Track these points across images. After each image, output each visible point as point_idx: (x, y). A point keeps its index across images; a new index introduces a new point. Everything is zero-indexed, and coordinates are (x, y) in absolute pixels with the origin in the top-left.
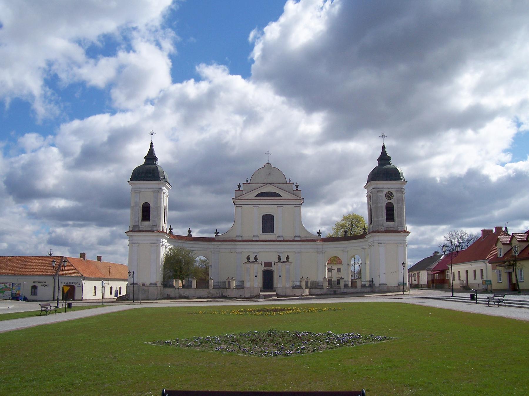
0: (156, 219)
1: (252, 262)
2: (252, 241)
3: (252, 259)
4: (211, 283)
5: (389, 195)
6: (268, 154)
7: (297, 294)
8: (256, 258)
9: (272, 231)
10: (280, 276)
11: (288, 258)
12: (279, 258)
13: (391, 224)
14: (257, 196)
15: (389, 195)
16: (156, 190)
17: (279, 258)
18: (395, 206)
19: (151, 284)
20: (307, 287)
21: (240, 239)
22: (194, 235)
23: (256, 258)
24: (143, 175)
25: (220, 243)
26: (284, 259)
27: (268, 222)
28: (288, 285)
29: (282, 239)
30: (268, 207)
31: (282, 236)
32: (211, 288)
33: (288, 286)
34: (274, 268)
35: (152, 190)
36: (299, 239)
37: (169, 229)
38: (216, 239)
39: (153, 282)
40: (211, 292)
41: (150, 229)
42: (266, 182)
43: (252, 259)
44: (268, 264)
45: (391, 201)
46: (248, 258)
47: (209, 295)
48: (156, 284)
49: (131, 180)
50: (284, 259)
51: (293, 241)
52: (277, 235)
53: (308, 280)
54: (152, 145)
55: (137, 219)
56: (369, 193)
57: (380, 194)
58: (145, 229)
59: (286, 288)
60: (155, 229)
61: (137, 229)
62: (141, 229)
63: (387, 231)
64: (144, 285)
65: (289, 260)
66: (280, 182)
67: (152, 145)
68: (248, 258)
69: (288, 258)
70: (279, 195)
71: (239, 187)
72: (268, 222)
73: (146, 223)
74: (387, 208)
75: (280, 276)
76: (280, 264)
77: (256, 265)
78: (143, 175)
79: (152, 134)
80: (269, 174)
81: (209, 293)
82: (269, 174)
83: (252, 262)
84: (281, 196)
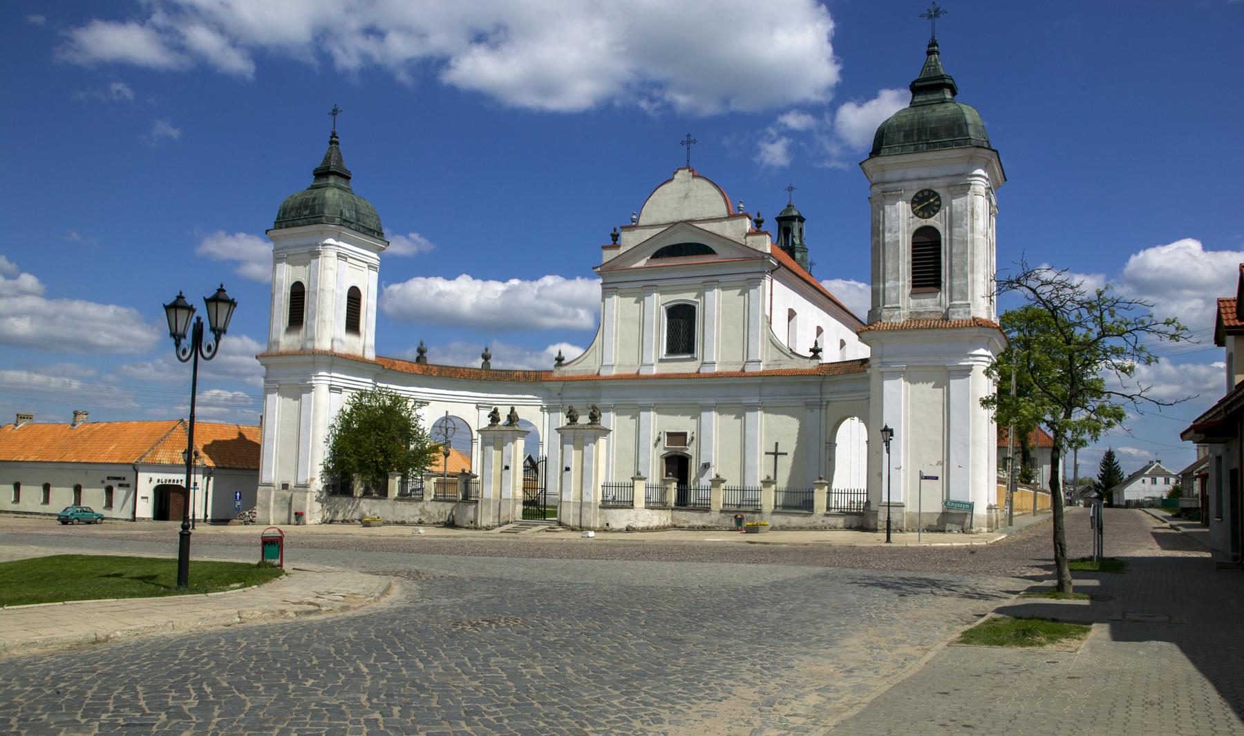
7: (614, 525)
14: (656, 256)
18: (944, 236)
27: (683, 329)
40: (428, 508)
47: (423, 519)
71: (615, 237)
72: (683, 329)
74: (915, 245)
81: (423, 512)
82: (686, 196)
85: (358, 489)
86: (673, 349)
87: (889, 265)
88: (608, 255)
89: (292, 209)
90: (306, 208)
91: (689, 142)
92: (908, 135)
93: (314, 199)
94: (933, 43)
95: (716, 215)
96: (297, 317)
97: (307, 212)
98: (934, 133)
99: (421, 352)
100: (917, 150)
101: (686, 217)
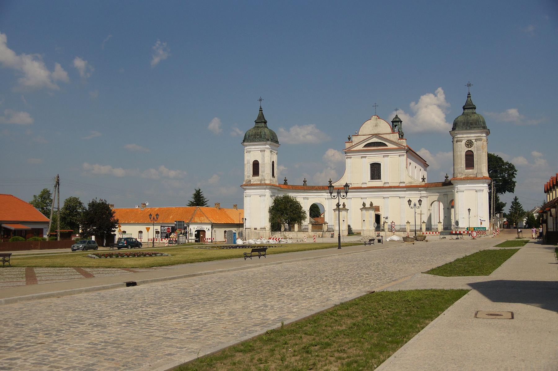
2: (361, 188)
5: (469, 143)
9: (379, 178)
14: (365, 146)
15: (469, 143)
17: (364, 204)
18: (475, 153)
19: (261, 228)
26: (368, 205)
27: (376, 171)
29: (387, 185)
30: (376, 158)
35: (260, 149)
41: (259, 182)
42: (372, 133)
45: (469, 149)
49: (244, 141)
52: (383, 182)
54: (261, 110)
57: (459, 143)
59: (370, 231)
60: (263, 182)
64: (255, 229)
66: (385, 132)
67: (261, 110)
71: (349, 139)
72: (376, 171)
73: (256, 178)
74: (466, 155)
76: (364, 211)
79: (260, 100)
80: (376, 126)
82: (376, 126)
84: (386, 145)
85: (283, 229)
87: (459, 161)
88: (348, 145)
90: (258, 135)
92: (464, 124)
93: (261, 132)
94: (469, 94)
95: (387, 132)
96: (256, 172)
98: (472, 124)
99: (285, 181)
100: (466, 129)
101: (376, 133)
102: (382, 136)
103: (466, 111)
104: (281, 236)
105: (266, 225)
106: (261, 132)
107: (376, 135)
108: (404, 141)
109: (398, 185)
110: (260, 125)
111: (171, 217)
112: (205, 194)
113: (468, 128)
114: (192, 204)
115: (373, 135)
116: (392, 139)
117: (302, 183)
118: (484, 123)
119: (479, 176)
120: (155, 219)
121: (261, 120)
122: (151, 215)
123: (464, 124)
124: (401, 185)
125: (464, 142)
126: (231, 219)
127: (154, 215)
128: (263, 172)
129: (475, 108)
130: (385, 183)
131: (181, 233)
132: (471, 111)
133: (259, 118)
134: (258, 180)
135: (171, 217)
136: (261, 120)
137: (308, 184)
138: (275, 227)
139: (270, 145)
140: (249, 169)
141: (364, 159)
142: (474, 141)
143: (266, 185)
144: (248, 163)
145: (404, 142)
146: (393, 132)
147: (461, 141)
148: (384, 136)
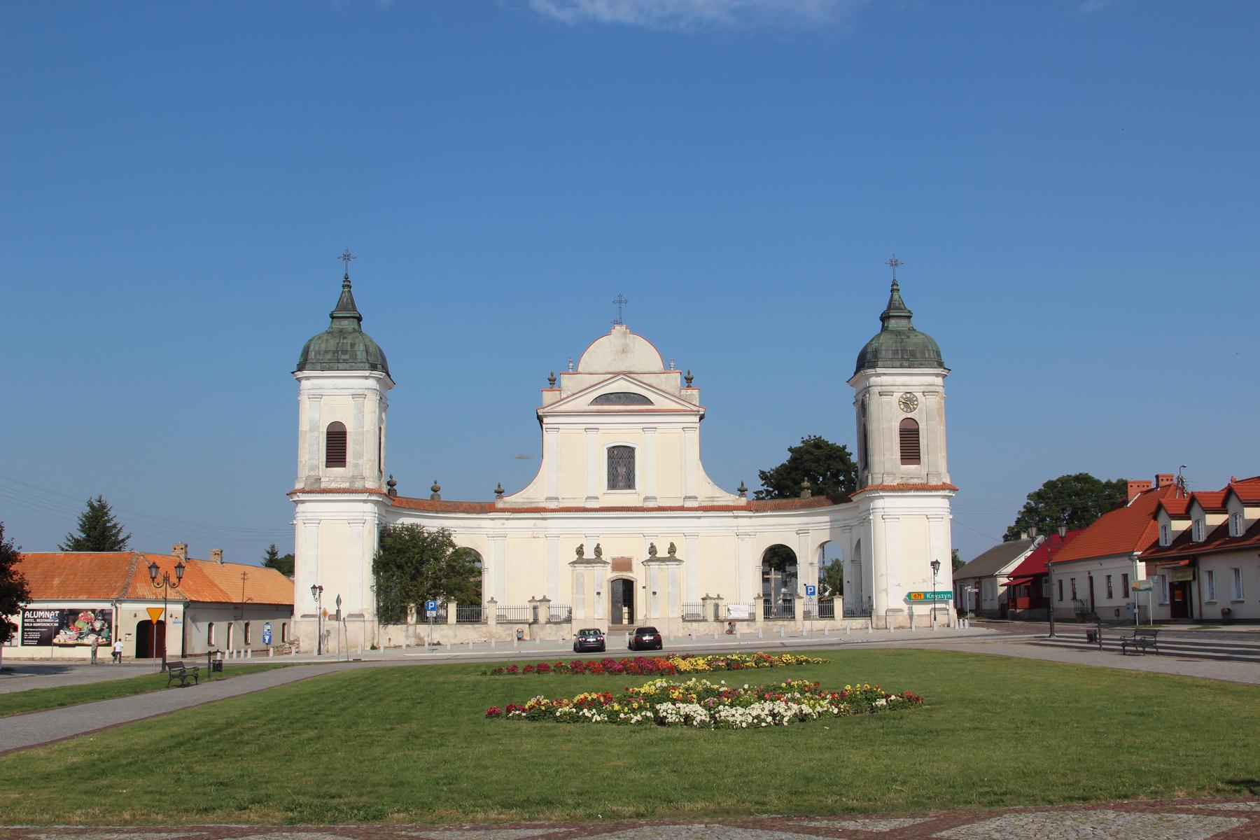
0: (361, 462)
1: (589, 562)
3: (589, 554)
4: (489, 611)
5: (908, 402)
6: (620, 302)
8: (598, 551)
9: (630, 484)
10: (654, 593)
11: (672, 549)
12: (653, 550)
13: (912, 468)
14: (597, 401)
15: (908, 402)
16: (360, 392)
17: (653, 550)
18: (922, 427)
20: (717, 619)
21: (553, 505)
22: (445, 495)
23: (598, 551)
24: (329, 356)
25: (507, 515)
26: (662, 552)
27: (621, 465)
28: (677, 613)
29: (651, 504)
31: (655, 498)
32: (492, 622)
33: (671, 616)
34: (638, 575)
36: (695, 504)
37: (389, 484)
38: (500, 505)
39: (357, 612)
41: (346, 485)
43: (589, 554)
44: (623, 564)
45: (909, 415)
46: (580, 551)
48: (362, 615)
50: (662, 552)
51: (682, 509)
53: (719, 602)
54: (347, 285)
55: (315, 462)
56: (860, 397)
57: (884, 398)
58: (333, 486)
59: (670, 620)
60: (358, 485)
61: (316, 487)
62: (323, 486)
63: (904, 488)
65: (677, 555)
66: (646, 370)
67: (347, 285)
68: (580, 551)
69: (672, 549)
70: (647, 401)
71: (552, 381)
72: (621, 465)
75: (654, 593)
76: (654, 566)
77: (598, 569)
78: (329, 356)
79: (347, 257)
80: (623, 351)
82: (623, 351)
83: (589, 562)
84: (650, 403)
86: (613, 484)
88: (548, 397)
89: (326, 352)
90: (345, 352)
91: (620, 302)
95: (653, 370)
97: (347, 357)
98: (913, 354)
100: (901, 367)
101: (623, 369)
102: (639, 377)
103: (893, 324)
104: (407, 637)
105: (366, 606)
106: (353, 345)
107: (627, 374)
108: (696, 392)
109: (679, 504)
110: (345, 324)
111: (56, 582)
112: (119, 516)
113: (906, 364)
114: (78, 546)
115: (618, 374)
116: (663, 387)
117: (427, 494)
118: (938, 354)
119: (933, 482)
120: (173, 579)
121: (347, 311)
122: (154, 566)
123: (895, 352)
124: (689, 504)
125: (897, 395)
126: (221, 591)
127: (167, 567)
128: (359, 455)
129: (909, 317)
130: (646, 499)
131: (93, 631)
132: (904, 322)
133: (341, 306)
134: (343, 479)
135: (56, 582)
136: (347, 311)
137: (445, 495)
138: (389, 613)
139: (379, 380)
140: (313, 449)
141: (591, 434)
142: (919, 395)
143: (365, 491)
144: (312, 430)
145: (694, 394)
146: (667, 369)
147: (890, 393)
148: (646, 378)
